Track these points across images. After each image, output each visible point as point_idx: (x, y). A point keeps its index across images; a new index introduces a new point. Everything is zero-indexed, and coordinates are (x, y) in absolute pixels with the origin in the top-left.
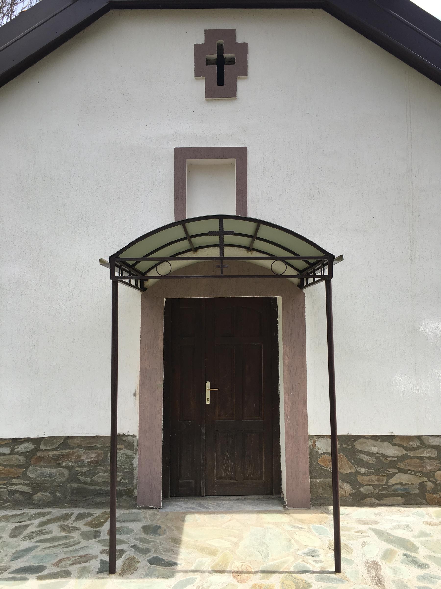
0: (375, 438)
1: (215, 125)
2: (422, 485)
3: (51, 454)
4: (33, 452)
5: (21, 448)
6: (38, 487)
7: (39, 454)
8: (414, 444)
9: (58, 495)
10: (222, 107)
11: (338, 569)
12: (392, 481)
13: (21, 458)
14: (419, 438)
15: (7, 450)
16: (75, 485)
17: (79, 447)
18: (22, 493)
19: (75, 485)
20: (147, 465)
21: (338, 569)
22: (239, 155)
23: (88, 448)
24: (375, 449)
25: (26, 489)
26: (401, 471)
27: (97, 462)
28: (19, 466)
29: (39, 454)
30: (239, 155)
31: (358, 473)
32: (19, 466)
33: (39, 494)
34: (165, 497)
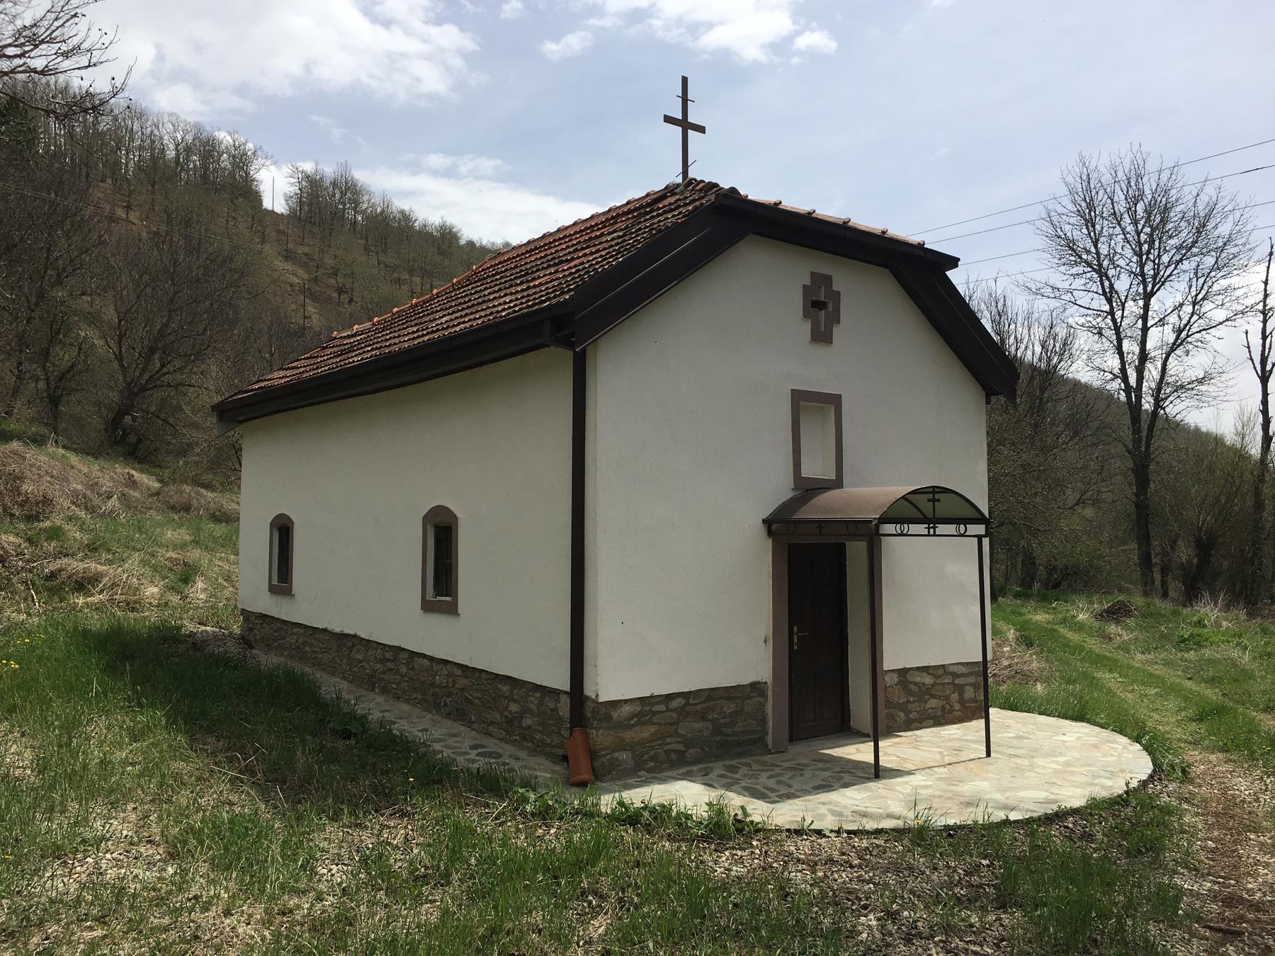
0: (918, 669)
1: (818, 370)
2: (943, 707)
3: (698, 707)
4: (640, 715)
5: (675, 704)
6: (689, 744)
7: (688, 709)
8: (941, 672)
9: (1039, 687)
10: (821, 350)
11: (988, 754)
12: (928, 706)
13: (674, 715)
14: (943, 666)
15: (662, 708)
16: (718, 738)
17: (722, 698)
18: (676, 752)
19: (718, 738)
20: (774, 710)
21: (988, 754)
22: (835, 400)
23: (729, 699)
24: (918, 679)
25: (680, 747)
26: (933, 697)
27: (736, 712)
28: (672, 724)
29: (688, 709)
30: (835, 400)
31: (909, 701)
32: (672, 724)
33: (691, 751)
34: (791, 740)
